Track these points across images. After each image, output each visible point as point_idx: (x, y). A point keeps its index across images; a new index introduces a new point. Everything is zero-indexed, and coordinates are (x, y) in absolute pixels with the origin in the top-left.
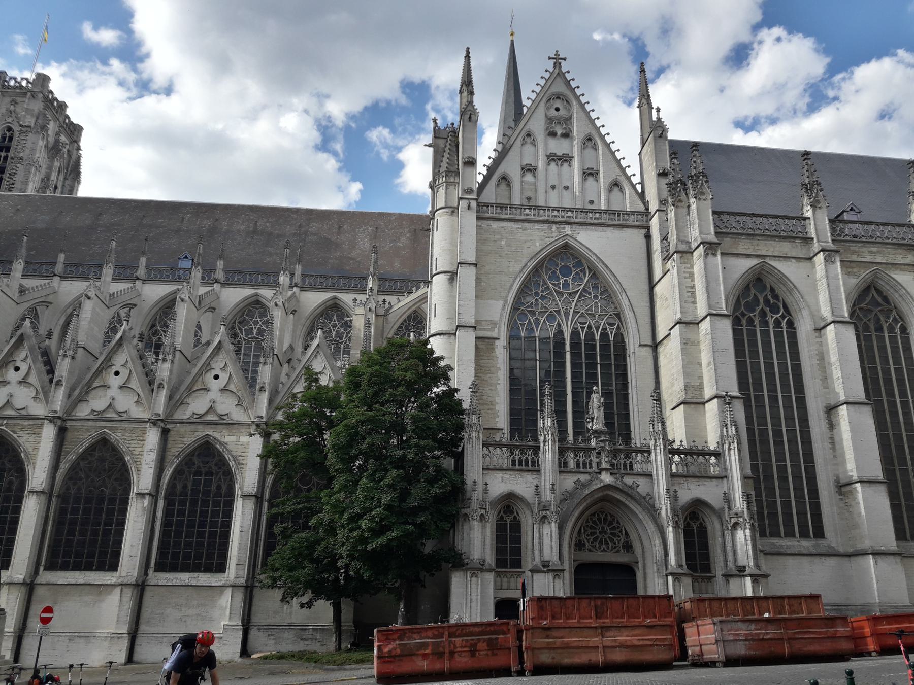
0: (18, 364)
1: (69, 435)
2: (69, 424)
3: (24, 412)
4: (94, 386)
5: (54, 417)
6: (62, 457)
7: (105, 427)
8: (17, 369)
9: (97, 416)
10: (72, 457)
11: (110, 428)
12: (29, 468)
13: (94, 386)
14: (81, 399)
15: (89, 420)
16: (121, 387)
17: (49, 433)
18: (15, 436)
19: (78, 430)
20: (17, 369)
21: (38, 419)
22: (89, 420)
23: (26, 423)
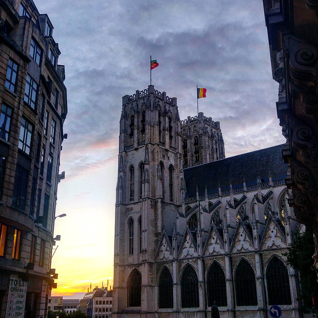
0: (214, 237)
1: (233, 260)
2: (232, 256)
3: (219, 253)
4: (236, 241)
5: (227, 254)
6: (233, 267)
7: (242, 255)
8: (214, 239)
9: (239, 252)
10: (235, 267)
11: (244, 256)
12: (225, 272)
13: (236, 241)
14: (233, 247)
15: (237, 253)
16: (244, 240)
17: (227, 259)
18: (218, 261)
19: (235, 257)
20: (214, 239)
21: (223, 255)
22: (237, 253)
23: (220, 257)
